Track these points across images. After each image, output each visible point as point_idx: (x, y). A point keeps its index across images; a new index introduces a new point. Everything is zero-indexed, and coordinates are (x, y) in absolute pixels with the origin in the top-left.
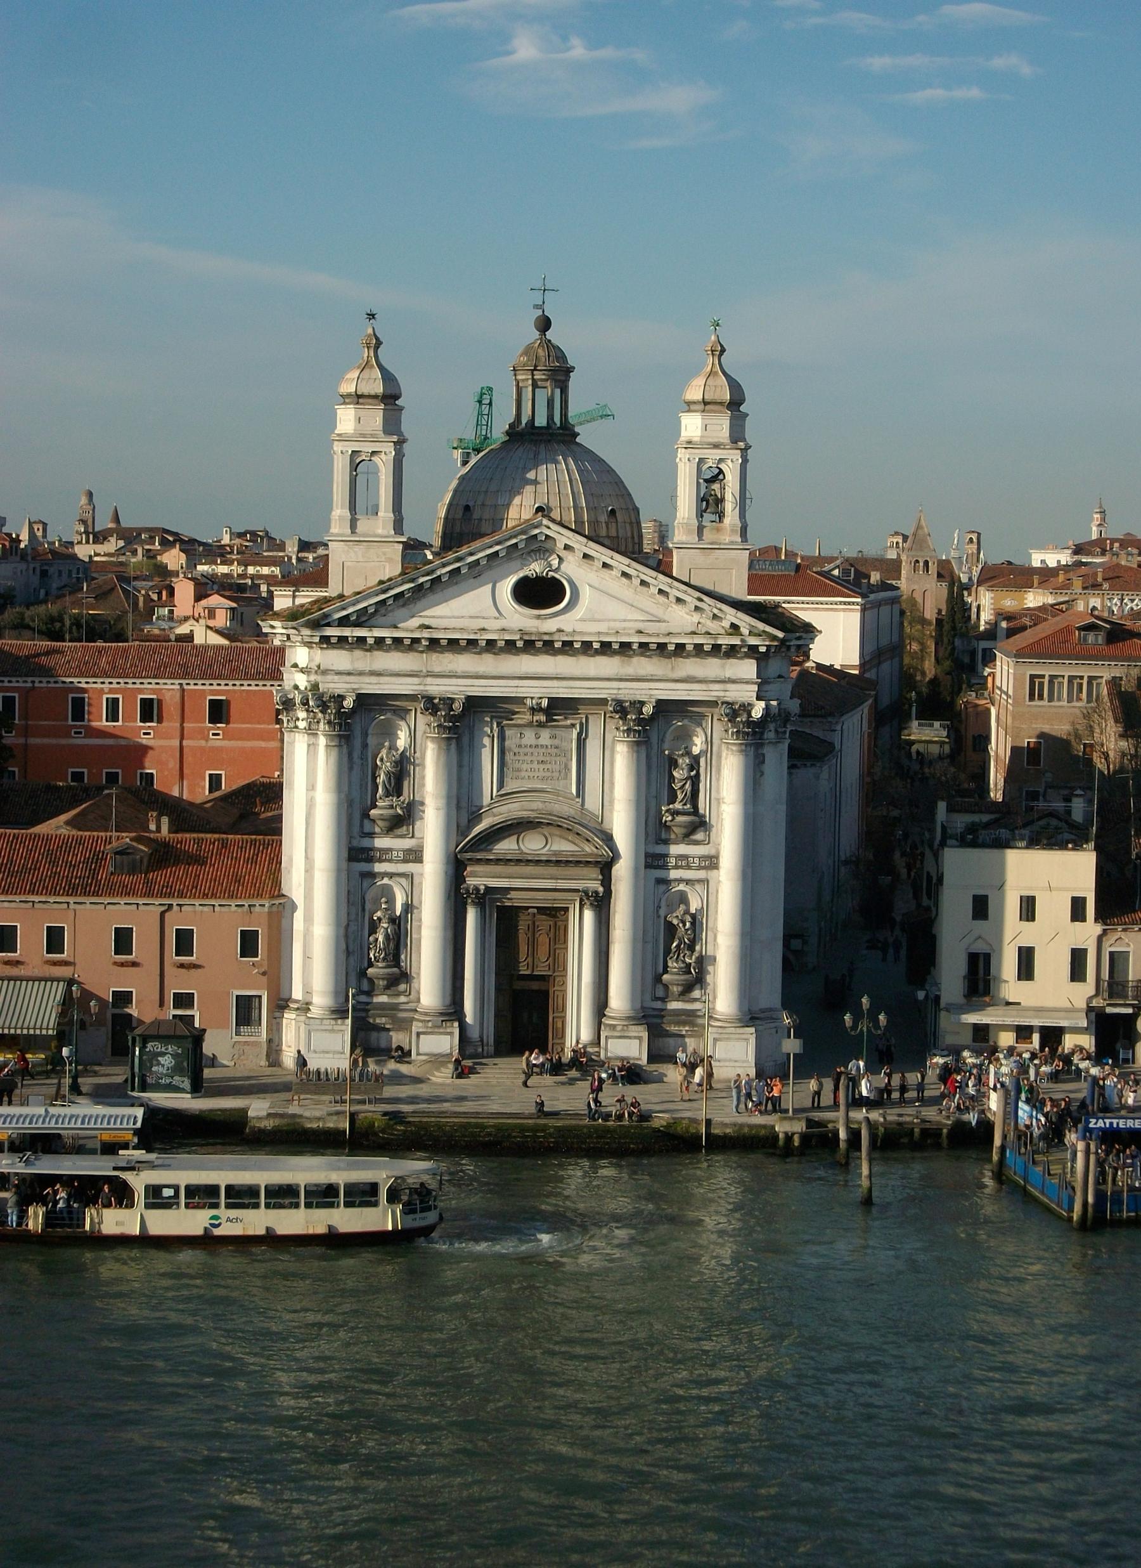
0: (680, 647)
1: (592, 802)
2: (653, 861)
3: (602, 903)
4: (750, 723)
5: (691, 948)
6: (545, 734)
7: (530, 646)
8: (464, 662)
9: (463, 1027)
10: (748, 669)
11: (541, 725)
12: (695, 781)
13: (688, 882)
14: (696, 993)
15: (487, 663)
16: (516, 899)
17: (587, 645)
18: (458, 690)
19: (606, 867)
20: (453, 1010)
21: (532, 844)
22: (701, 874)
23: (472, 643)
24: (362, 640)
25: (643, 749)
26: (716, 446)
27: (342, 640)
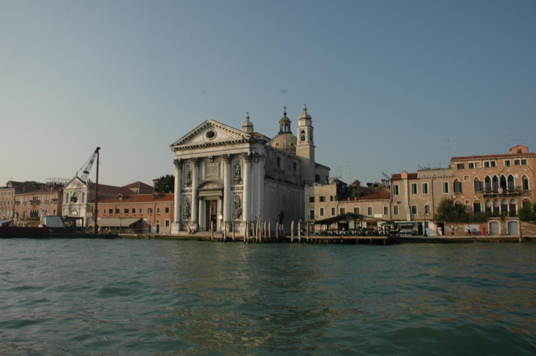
0: (233, 141)
1: (222, 178)
2: (232, 189)
3: (222, 198)
4: (248, 157)
5: (240, 206)
6: (213, 164)
7: (209, 145)
8: (198, 151)
9: (198, 224)
10: (248, 145)
11: (212, 162)
12: (240, 171)
13: (239, 193)
14: (241, 217)
15: (202, 150)
16: (208, 198)
17: (217, 143)
18: (196, 156)
19: (222, 190)
20: (197, 222)
21: (210, 186)
22: (241, 191)
23: (198, 146)
24: (180, 148)
25: (229, 165)
26: (303, 126)
27: (177, 148)
